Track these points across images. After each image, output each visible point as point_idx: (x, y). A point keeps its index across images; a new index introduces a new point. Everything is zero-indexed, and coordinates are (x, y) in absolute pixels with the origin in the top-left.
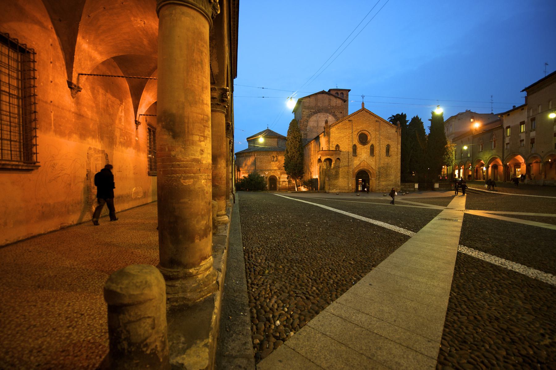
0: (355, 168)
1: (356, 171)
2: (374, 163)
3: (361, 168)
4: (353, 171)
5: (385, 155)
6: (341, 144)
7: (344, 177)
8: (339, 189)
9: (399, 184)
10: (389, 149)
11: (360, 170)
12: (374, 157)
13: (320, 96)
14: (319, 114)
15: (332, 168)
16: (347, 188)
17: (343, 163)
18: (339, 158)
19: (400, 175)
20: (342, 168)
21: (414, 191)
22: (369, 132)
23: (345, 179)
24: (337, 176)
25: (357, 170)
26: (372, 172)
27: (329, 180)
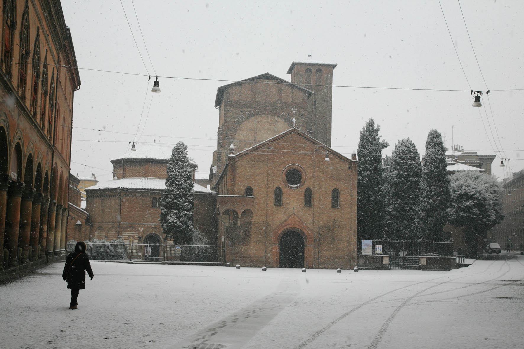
1: (279, 232)
3: (288, 226)
5: (330, 206)
6: (255, 186)
8: (250, 262)
10: (337, 197)
11: (287, 229)
12: (312, 209)
13: (261, 84)
14: (257, 119)
15: (239, 225)
20: (256, 225)
22: (302, 169)
23: (261, 245)
25: (283, 229)
27: (233, 244)
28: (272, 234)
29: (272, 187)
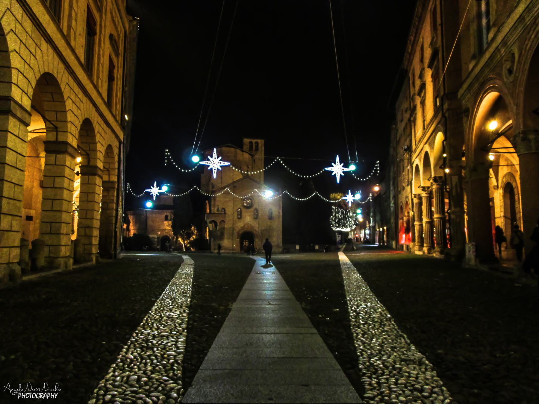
0: (240, 230)
1: (240, 233)
2: (257, 225)
3: (245, 230)
4: (238, 233)
7: (228, 238)
9: (281, 245)
12: (258, 220)
15: (218, 229)
16: (231, 248)
17: (228, 225)
18: (224, 220)
19: (282, 237)
21: (296, 252)
24: (221, 237)
26: (255, 233)
27: (214, 240)
28: (236, 234)
29: (236, 208)
